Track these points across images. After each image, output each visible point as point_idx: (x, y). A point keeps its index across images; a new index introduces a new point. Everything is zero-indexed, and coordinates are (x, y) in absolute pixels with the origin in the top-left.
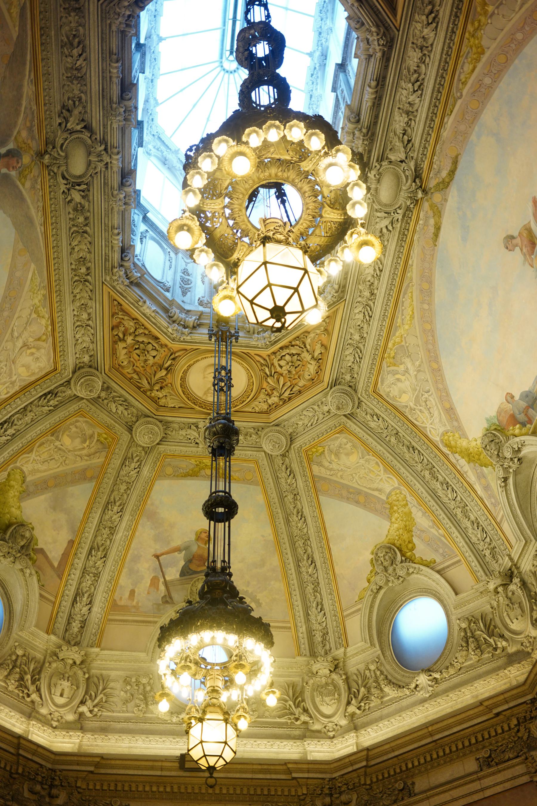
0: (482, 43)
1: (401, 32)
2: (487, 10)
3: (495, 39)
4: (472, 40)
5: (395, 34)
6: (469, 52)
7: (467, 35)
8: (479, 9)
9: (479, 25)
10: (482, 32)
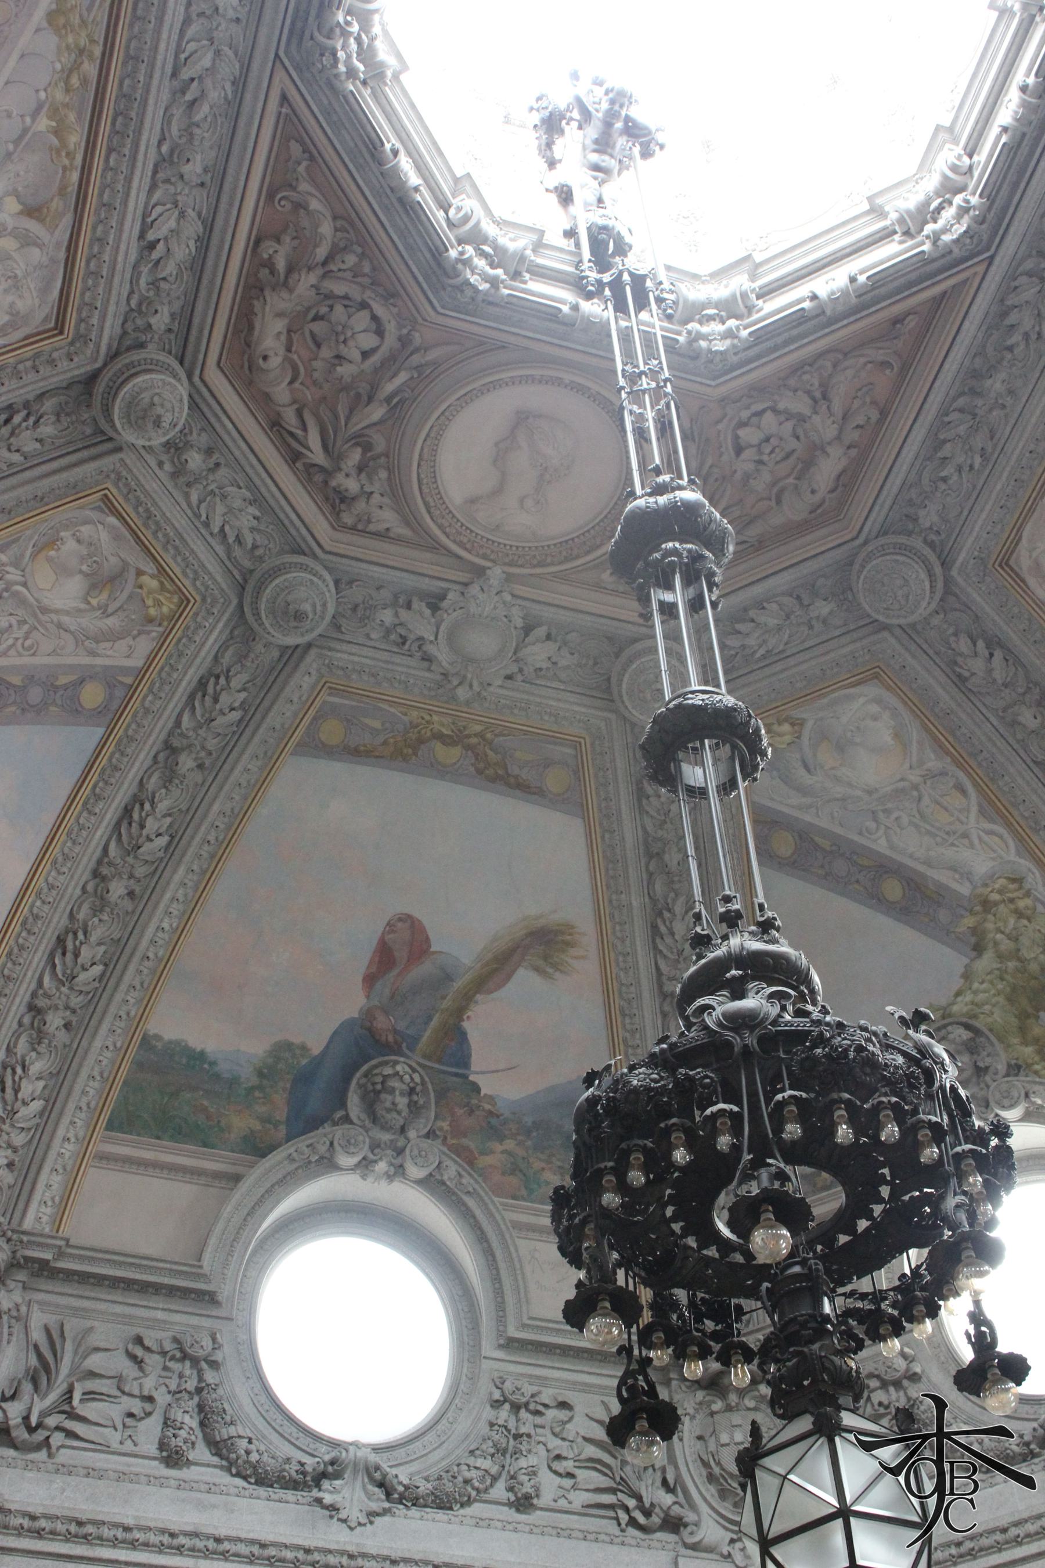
0: (56, 39)
1: (272, 56)
2: (50, 118)
3: (22, 56)
4: (83, 41)
5: (286, 53)
6: (89, 10)
7: (98, 51)
8: (72, 117)
9: (67, 81)
10: (58, 66)
